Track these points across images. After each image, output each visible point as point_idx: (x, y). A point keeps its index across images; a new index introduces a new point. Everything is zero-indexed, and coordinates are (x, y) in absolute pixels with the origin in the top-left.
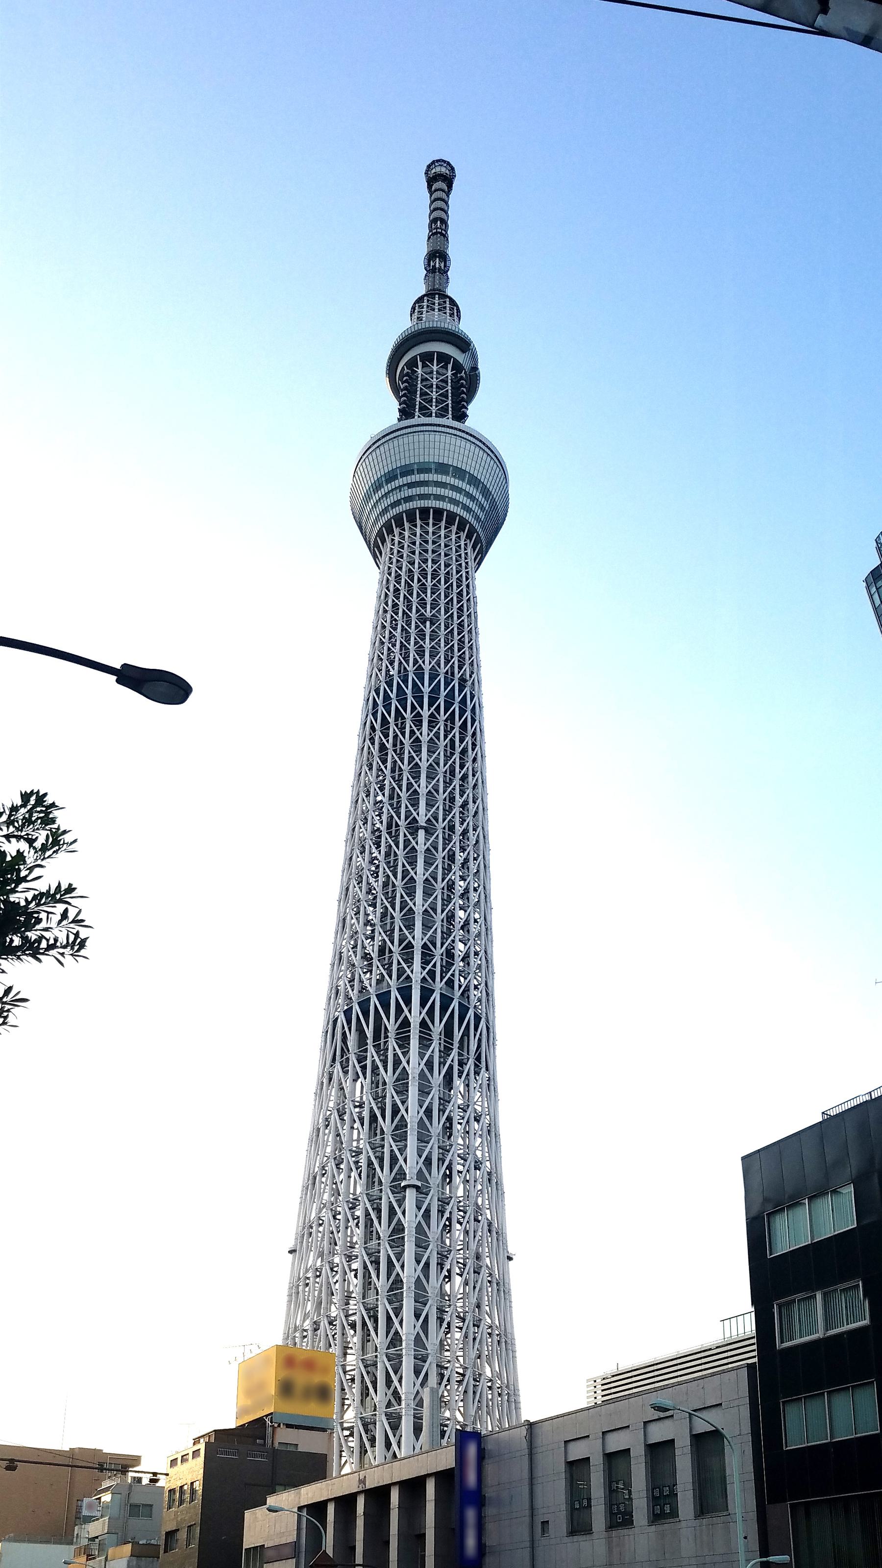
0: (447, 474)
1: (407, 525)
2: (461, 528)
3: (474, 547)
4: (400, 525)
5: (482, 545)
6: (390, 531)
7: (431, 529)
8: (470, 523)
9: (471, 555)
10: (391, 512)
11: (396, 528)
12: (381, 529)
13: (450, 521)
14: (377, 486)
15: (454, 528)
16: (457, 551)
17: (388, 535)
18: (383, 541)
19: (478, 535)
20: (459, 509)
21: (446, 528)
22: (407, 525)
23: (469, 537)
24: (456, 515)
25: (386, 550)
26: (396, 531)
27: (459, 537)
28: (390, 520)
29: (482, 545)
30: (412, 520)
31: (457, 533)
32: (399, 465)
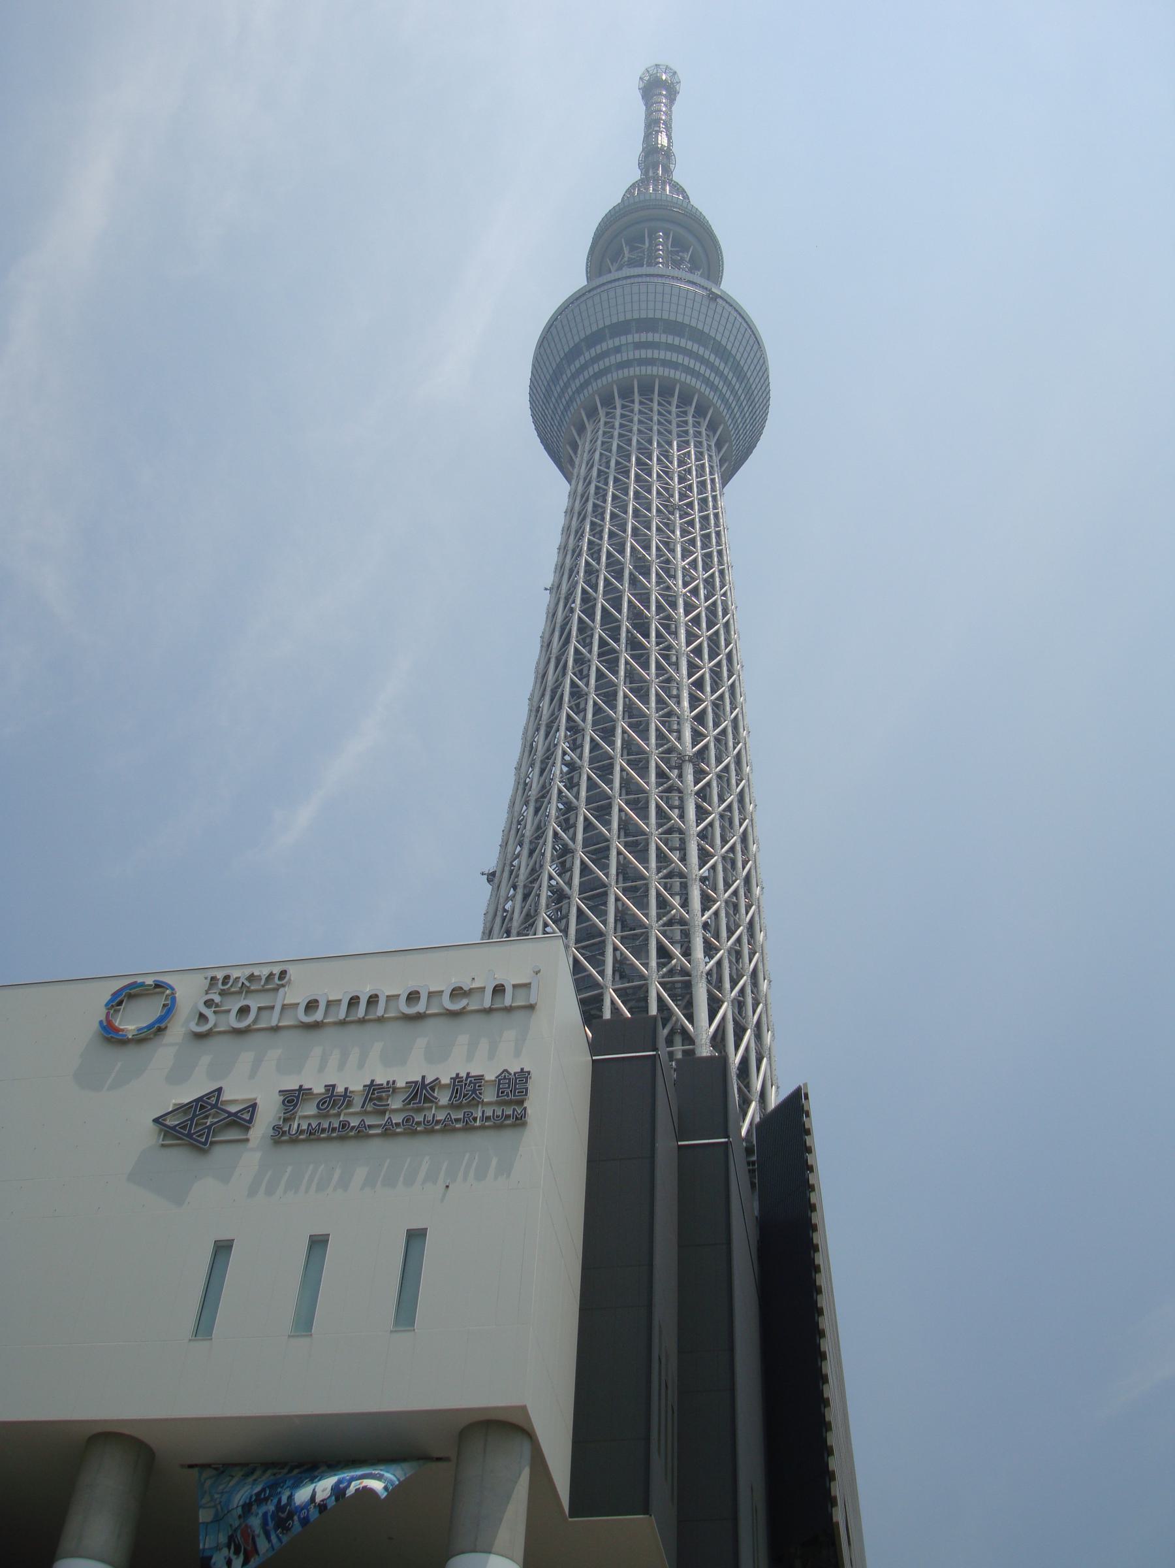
0: (681, 335)
3: (719, 446)
4: (608, 402)
5: (731, 446)
6: (592, 413)
8: (715, 406)
10: (594, 384)
13: (685, 400)
14: (574, 353)
15: (691, 410)
17: (589, 421)
18: (581, 429)
20: (699, 383)
23: (712, 427)
25: (585, 445)
26: (602, 412)
27: (699, 423)
29: (731, 446)
30: (626, 393)
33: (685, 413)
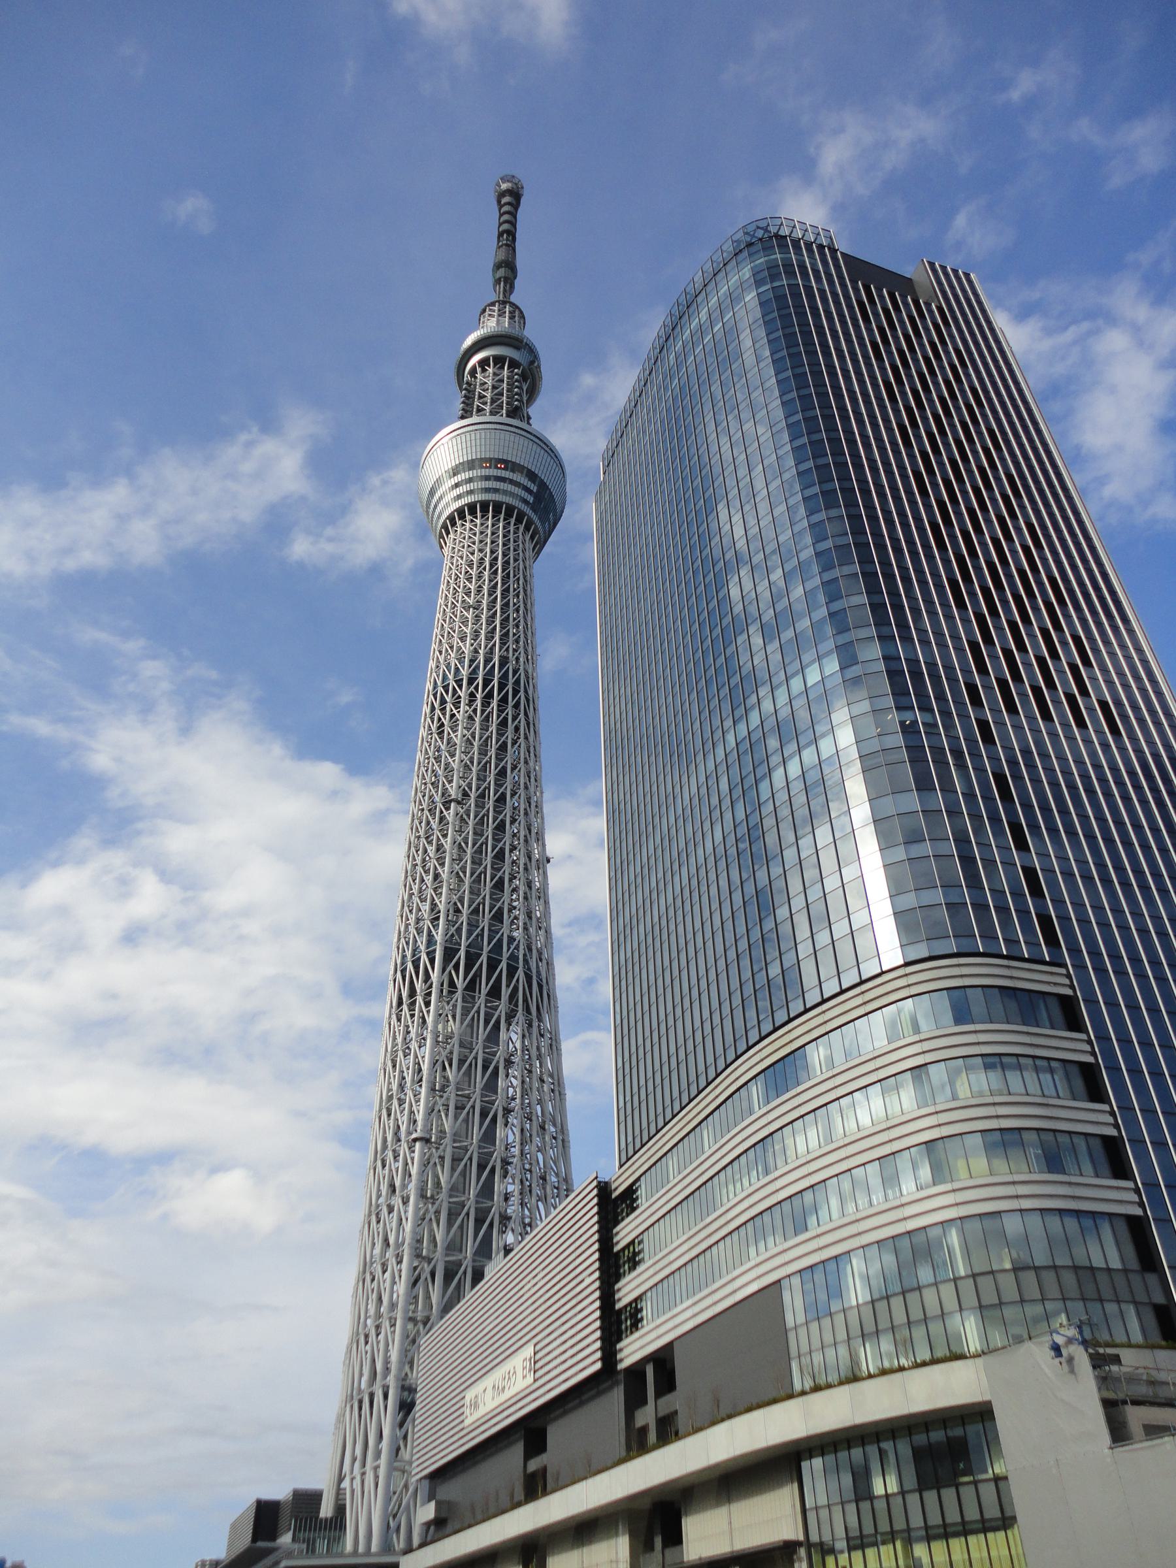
1: (468, 517)
2: (519, 521)
3: (532, 538)
5: (540, 536)
6: (454, 524)
7: (490, 523)
8: (528, 515)
9: (529, 546)
11: (459, 520)
12: (445, 522)
15: (513, 521)
16: (515, 542)
18: (448, 533)
19: (536, 526)
21: (505, 520)
22: (468, 517)
23: (527, 528)
24: (514, 508)
26: (459, 523)
27: (518, 528)
28: (453, 513)
29: (540, 536)
31: (515, 525)
32: (461, 461)
33: (509, 523)
